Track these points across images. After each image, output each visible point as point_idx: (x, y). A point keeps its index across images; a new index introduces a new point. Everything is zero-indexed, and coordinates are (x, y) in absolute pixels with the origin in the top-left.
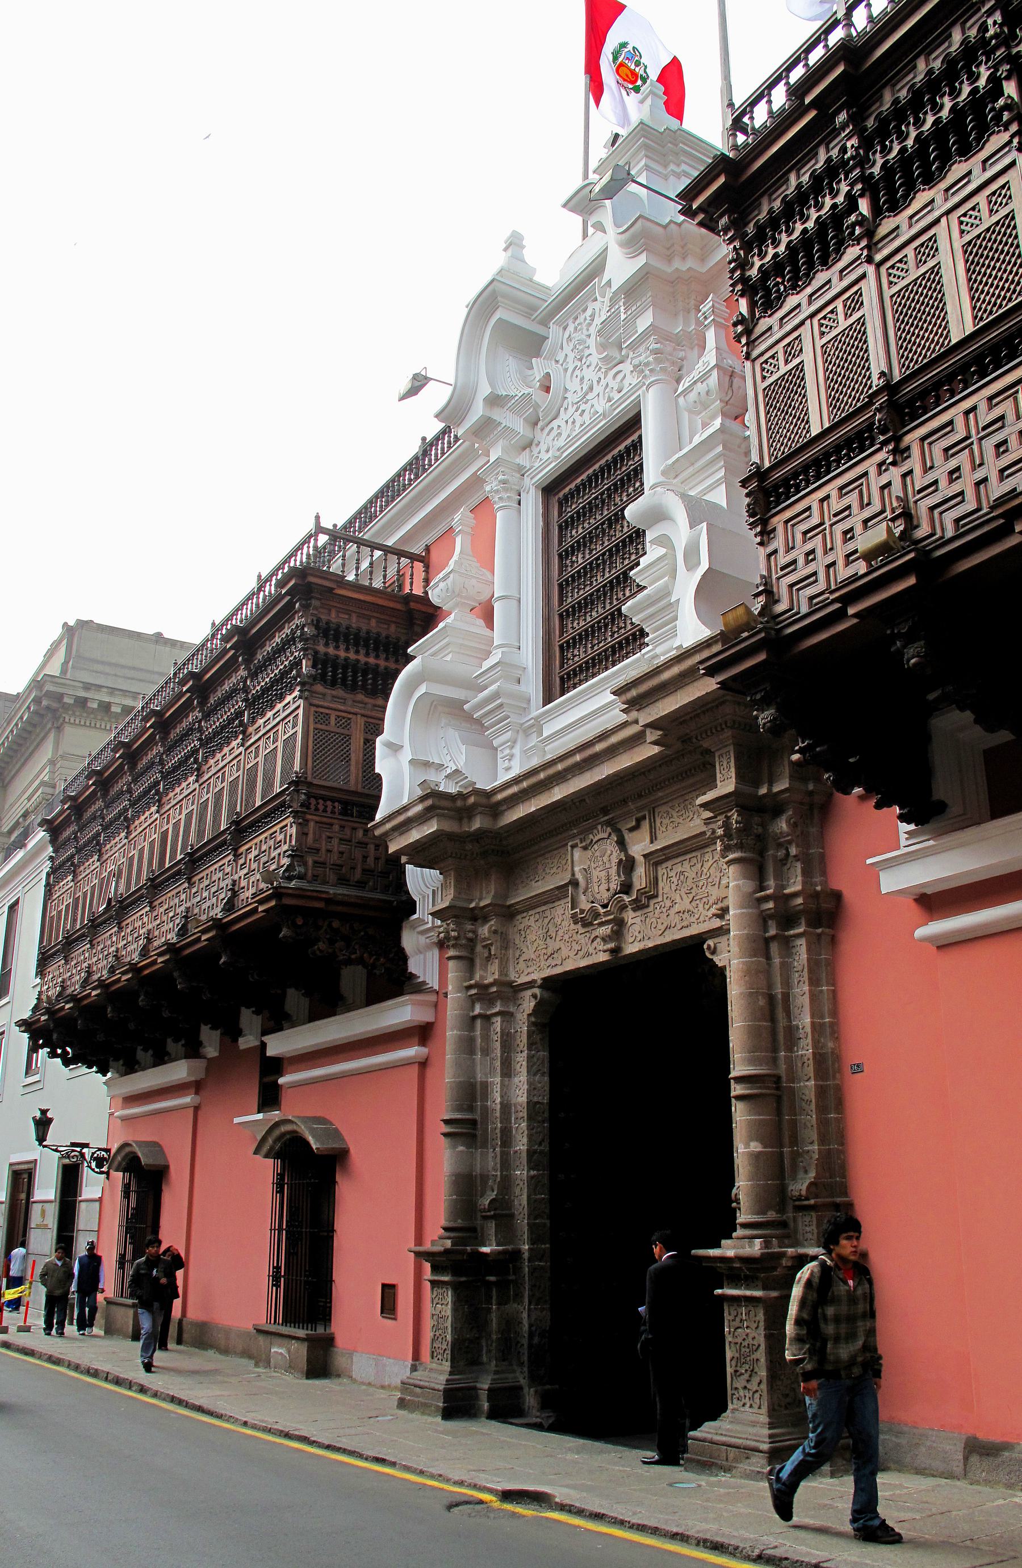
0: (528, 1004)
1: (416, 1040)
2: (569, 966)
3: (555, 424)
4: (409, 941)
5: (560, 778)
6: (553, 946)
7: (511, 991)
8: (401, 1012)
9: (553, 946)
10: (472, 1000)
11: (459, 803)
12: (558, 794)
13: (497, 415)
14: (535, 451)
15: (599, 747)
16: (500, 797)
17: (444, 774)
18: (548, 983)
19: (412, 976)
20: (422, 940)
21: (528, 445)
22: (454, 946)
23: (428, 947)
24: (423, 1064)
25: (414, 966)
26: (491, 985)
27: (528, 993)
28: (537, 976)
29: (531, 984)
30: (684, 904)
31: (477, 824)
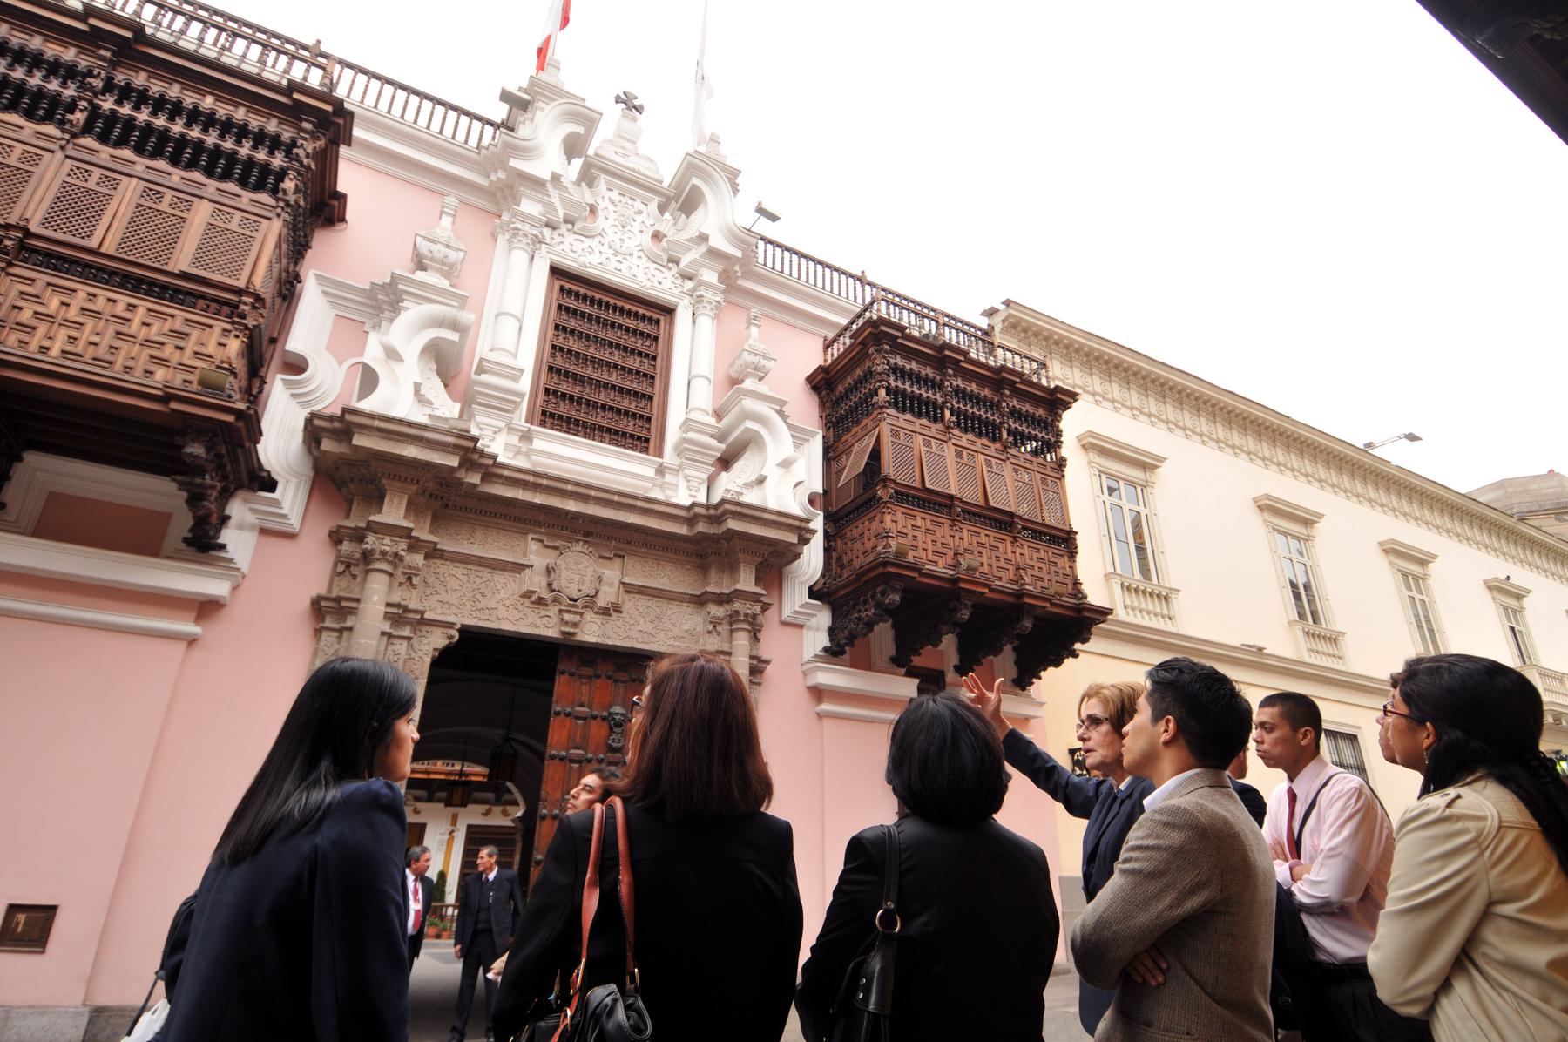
0: (438, 640)
1: (193, 615)
2: (506, 626)
3: (587, 242)
4: (238, 509)
5: (585, 498)
6: (484, 603)
7: (423, 622)
8: (210, 585)
9: (484, 603)
10: (387, 616)
11: (476, 457)
12: (572, 506)
13: (549, 186)
14: (556, 233)
15: (639, 504)
16: (506, 473)
17: (429, 411)
18: (465, 631)
19: (222, 547)
20: (251, 518)
21: (551, 226)
22: (389, 562)
23: (251, 528)
24: (192, 641)
25: (227, 536)
26: (416, 611)
27: (438, 631)
28: (459, 621)
29: (450, 625)
30: (649, 628)
31: (475, 478)
